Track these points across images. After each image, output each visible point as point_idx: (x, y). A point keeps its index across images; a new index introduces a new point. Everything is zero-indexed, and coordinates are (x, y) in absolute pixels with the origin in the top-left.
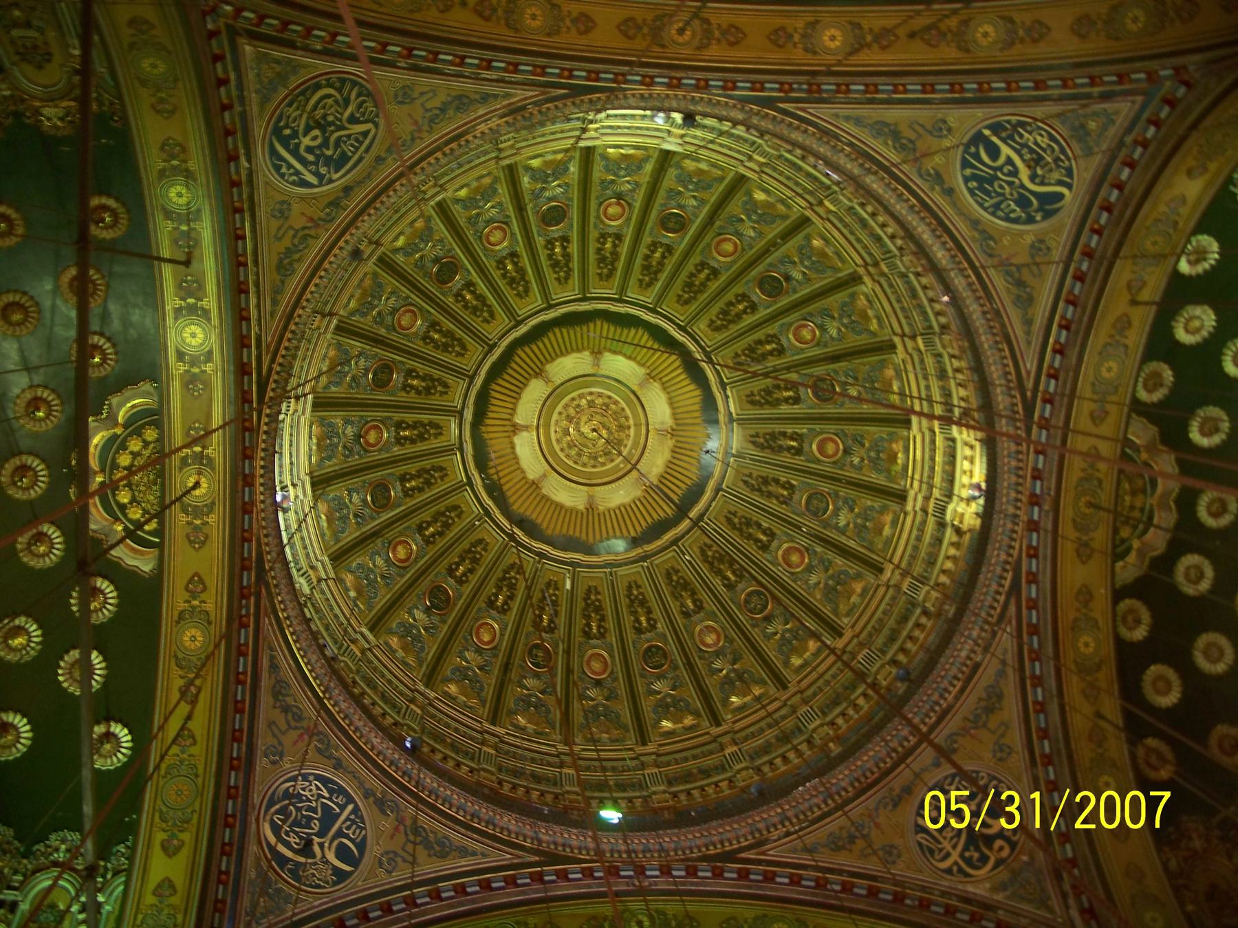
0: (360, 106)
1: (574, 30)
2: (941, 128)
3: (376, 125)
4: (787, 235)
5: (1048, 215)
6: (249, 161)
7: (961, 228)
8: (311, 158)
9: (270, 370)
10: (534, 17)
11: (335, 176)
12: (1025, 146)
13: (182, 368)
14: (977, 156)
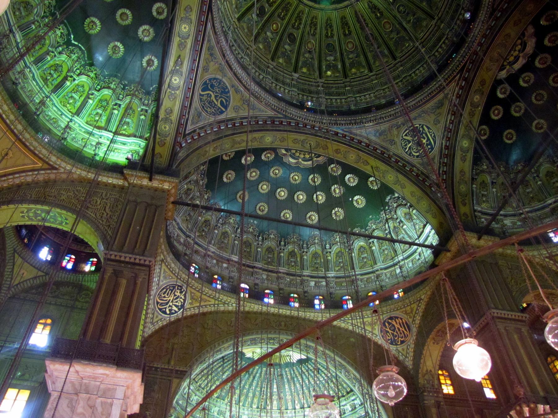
0: (406, 145)
1: (341, 151)
2: (236, 109)
3: (402, 136)
4: (258, 35)
5: (205, 83)
6: (442, 143)
7: (230, 74)
8: (424, 135)
9: (457, 74)
10: (352, 157)
11: (418, 125)
12: (213, 107)
13: (484, 90)
14: (226, 101)
